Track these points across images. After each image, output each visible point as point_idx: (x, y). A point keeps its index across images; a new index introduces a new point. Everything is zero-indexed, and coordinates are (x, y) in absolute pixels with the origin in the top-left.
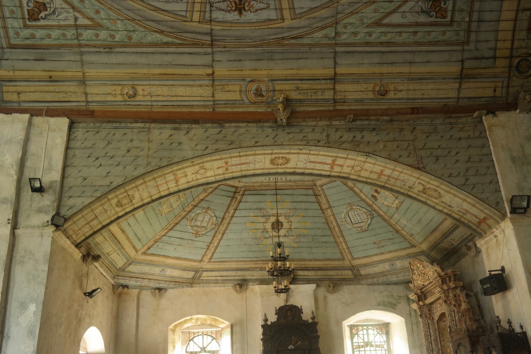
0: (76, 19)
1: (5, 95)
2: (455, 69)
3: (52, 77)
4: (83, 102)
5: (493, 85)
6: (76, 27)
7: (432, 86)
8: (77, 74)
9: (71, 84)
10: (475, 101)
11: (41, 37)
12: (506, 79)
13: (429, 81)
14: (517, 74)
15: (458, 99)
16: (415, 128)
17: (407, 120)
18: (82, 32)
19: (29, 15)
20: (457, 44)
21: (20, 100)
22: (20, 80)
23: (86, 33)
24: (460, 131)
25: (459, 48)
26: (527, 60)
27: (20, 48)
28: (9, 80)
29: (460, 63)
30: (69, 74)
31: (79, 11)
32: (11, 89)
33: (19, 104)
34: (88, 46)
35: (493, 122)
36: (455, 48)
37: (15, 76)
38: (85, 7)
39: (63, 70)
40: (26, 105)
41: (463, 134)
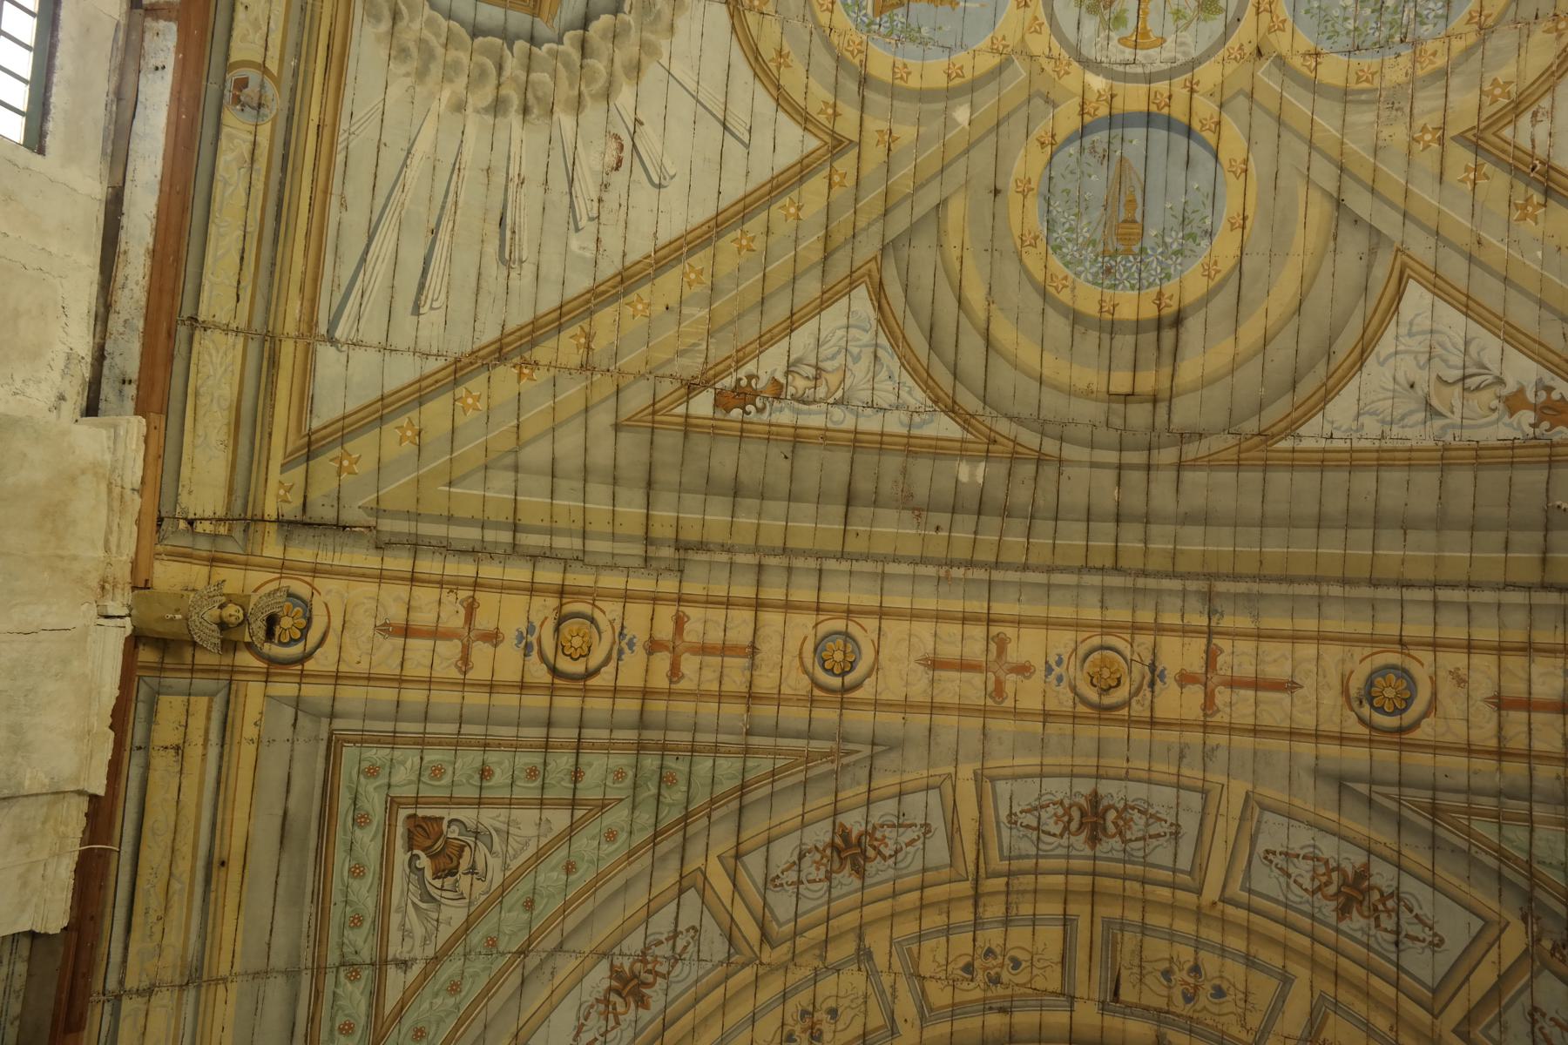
0: (404, 964)
1: (179, 701)
3: (223, 869)
4: (121, 982)
6: (380, 964)
8: (226, 957)
9: (193, 937)
11: (357, 847)
18: (363, 982)
19: (425, 818)
21: (154, 753)
22: (226, 758)
23: (357, 994)
27: (326, 771)
28: (230, 720)
30: (228, 930)
31: (425, 975)
32: (197, 724)
33: (140, 748)
34: (317, 998)
37: (239, 743)
38: (436, 995)
39: (243, 908)
40: (135, 772)
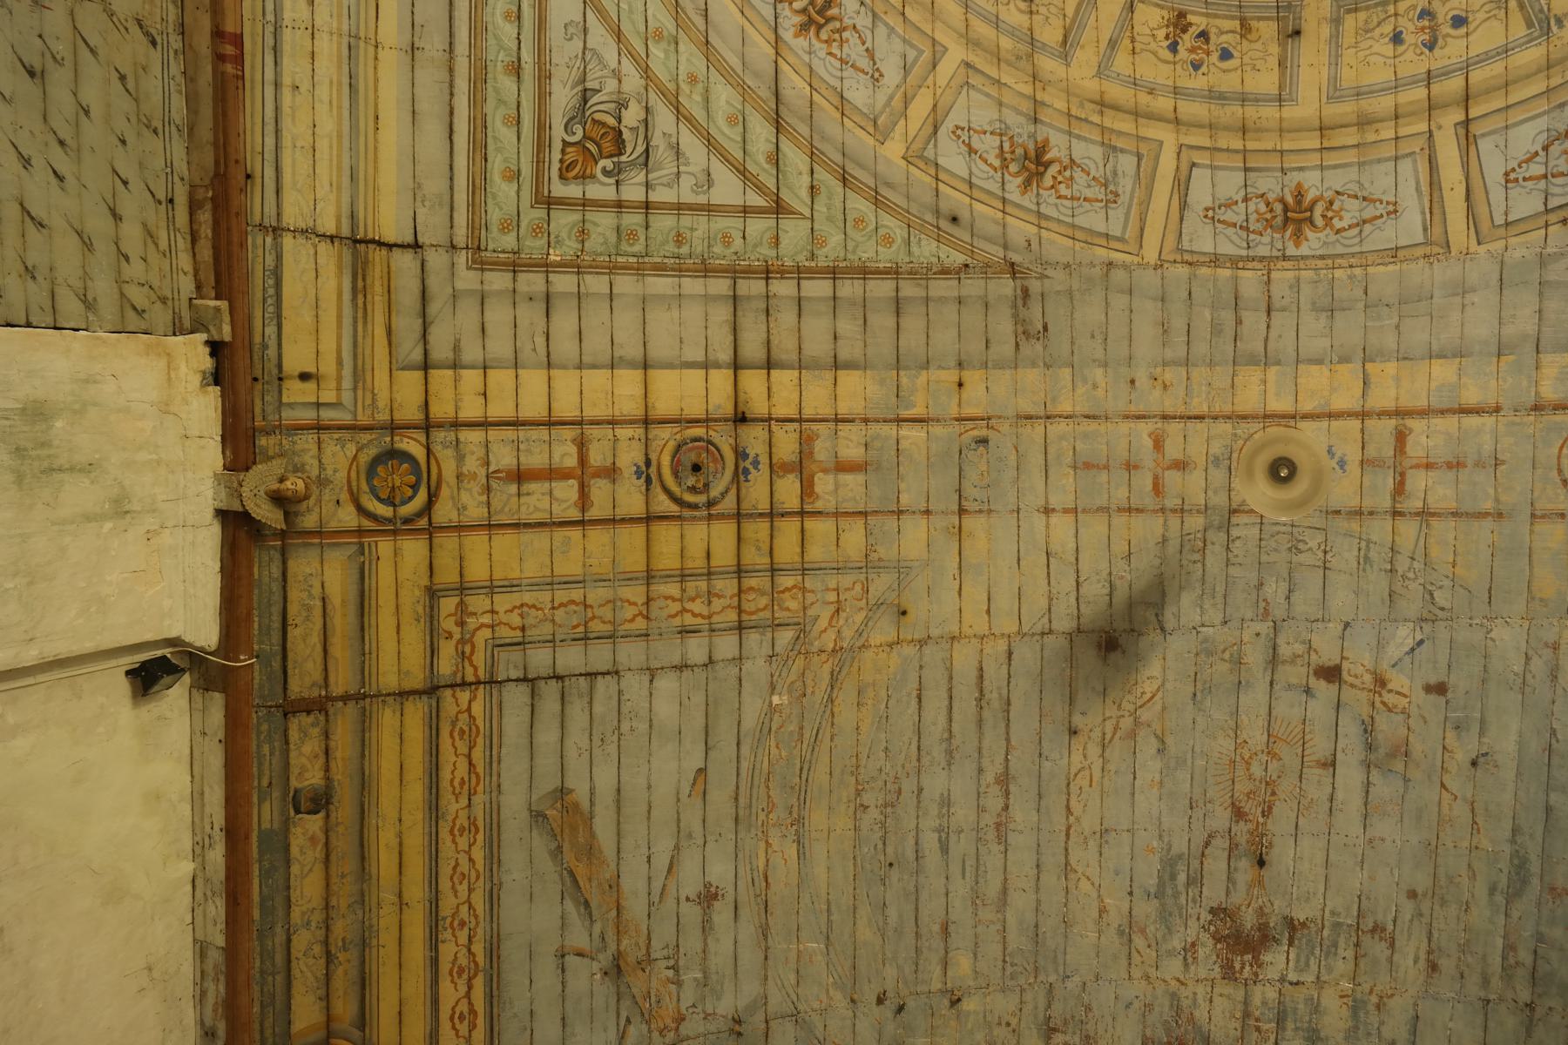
2: (391, 225)
5: (328, 367)
7: (327, 125)
10: (264, 300)
12: (344, 417)
13: (346, 113)
14: (365, 458)
15: (275, 230)
16: (154, 43)
17: (182, 30)
20: (472, 227)
24: (145, 225)
25: (461, 237)
26: (415, 487)
29: (409, 239)
35: (183, 369)
36: (461, 218)
41: (131, 232)
